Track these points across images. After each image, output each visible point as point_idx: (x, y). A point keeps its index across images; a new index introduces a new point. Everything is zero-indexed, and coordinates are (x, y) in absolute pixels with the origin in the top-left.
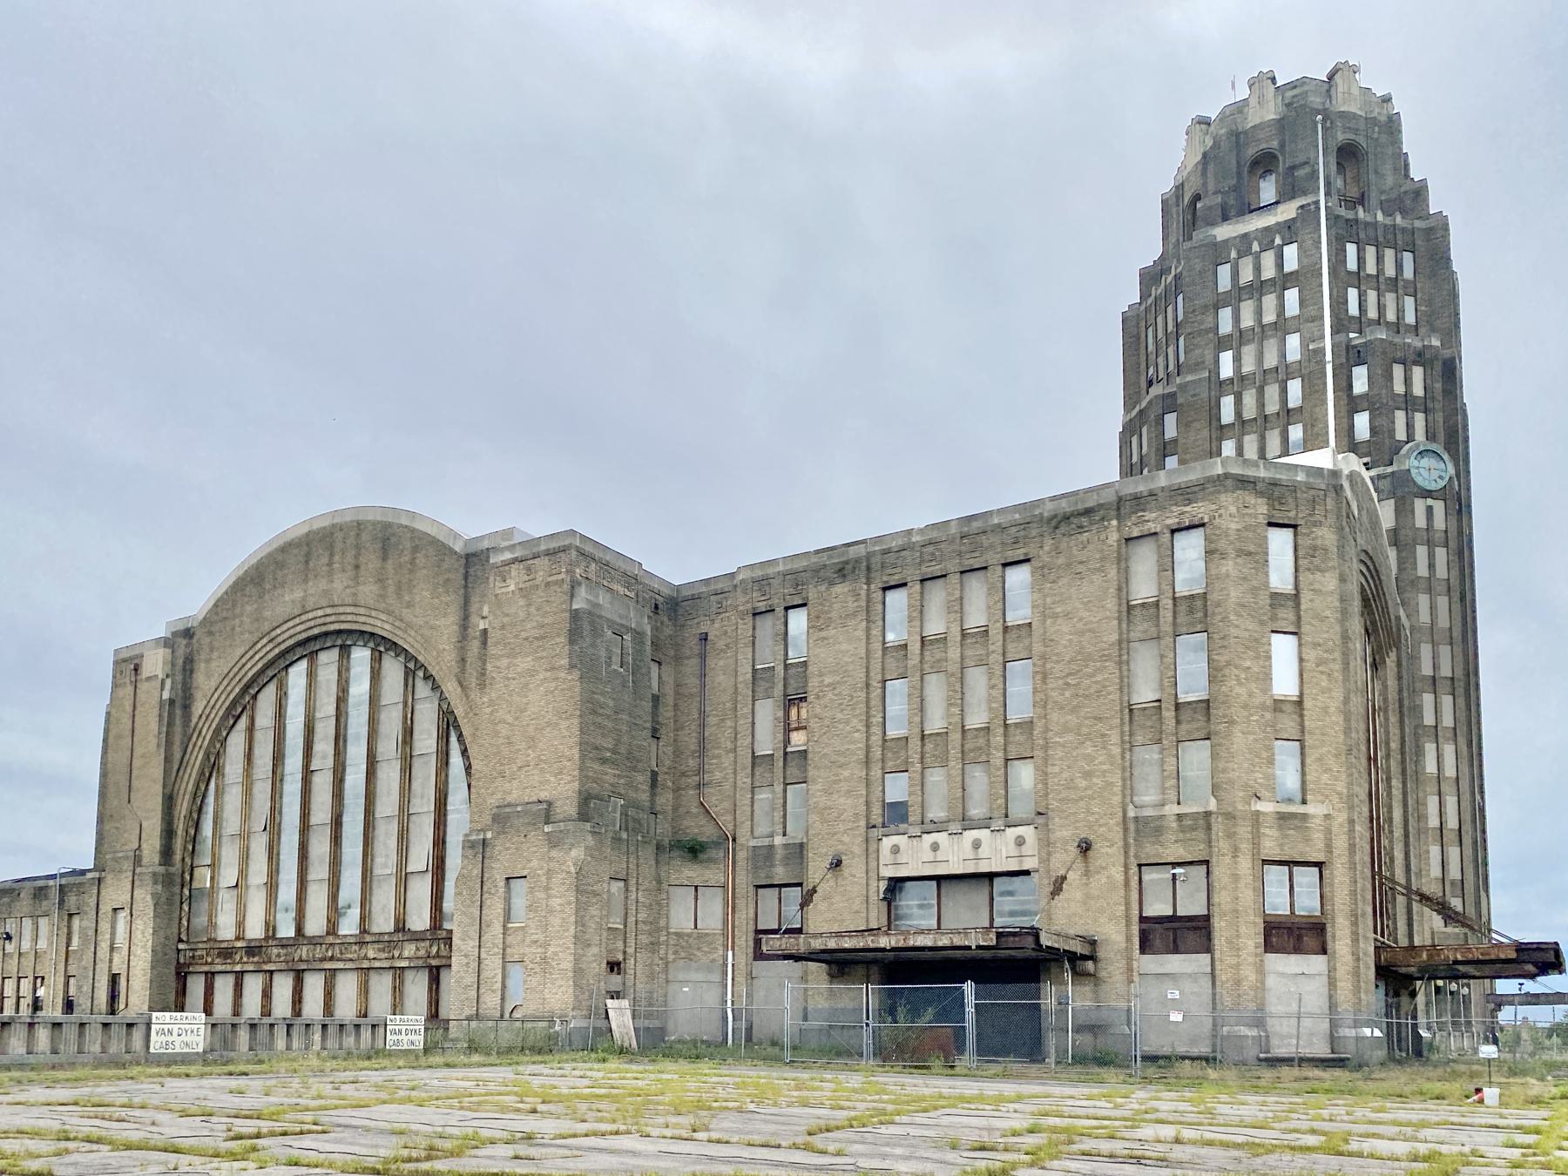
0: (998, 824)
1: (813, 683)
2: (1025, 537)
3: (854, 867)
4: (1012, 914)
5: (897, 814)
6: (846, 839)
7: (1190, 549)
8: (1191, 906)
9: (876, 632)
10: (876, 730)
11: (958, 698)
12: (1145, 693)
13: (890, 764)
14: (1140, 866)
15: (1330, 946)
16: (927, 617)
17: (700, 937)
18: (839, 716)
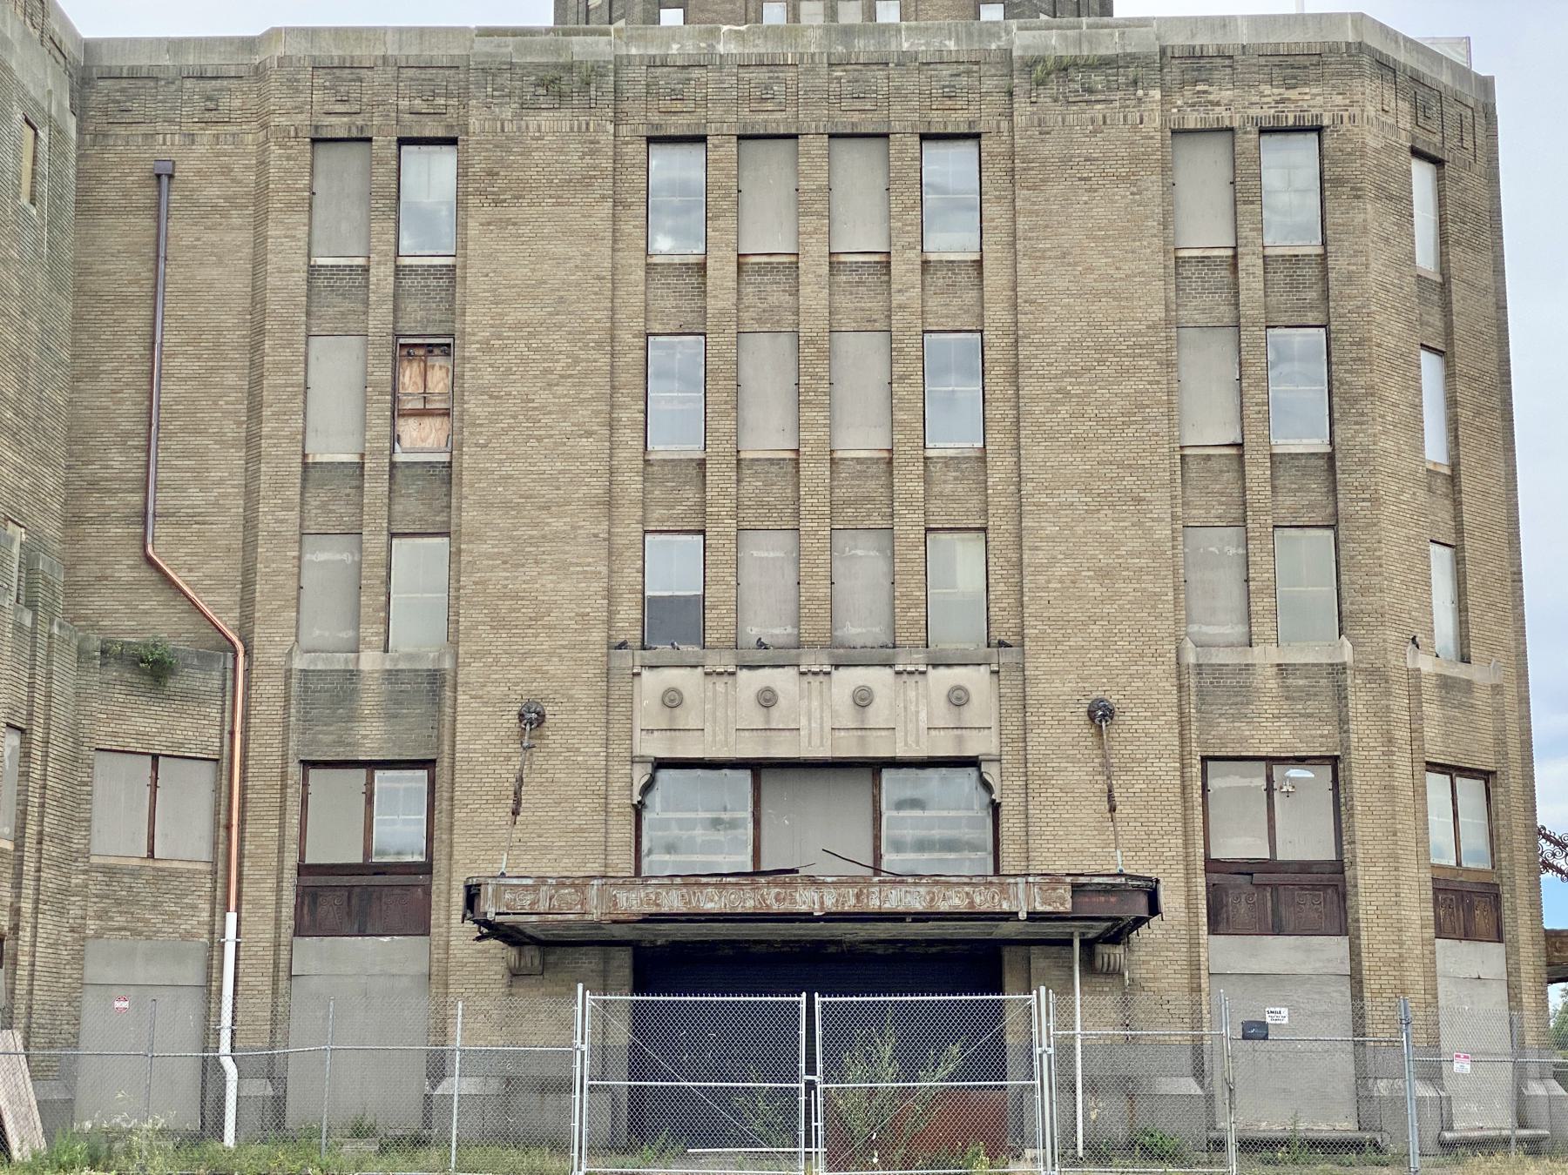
1: (476, 320)
2: (970, 88)
3: (575, 732)
4: (922, 846)
7: (1288, 171)
8: (1304, 839)
9: (631, 227)
10: (629, 437)
12: (1210, 426)
13: (658, 513)
14: (1204, 759)
15: (1507, 928)
17: (162, 876)
18: (542, 397)
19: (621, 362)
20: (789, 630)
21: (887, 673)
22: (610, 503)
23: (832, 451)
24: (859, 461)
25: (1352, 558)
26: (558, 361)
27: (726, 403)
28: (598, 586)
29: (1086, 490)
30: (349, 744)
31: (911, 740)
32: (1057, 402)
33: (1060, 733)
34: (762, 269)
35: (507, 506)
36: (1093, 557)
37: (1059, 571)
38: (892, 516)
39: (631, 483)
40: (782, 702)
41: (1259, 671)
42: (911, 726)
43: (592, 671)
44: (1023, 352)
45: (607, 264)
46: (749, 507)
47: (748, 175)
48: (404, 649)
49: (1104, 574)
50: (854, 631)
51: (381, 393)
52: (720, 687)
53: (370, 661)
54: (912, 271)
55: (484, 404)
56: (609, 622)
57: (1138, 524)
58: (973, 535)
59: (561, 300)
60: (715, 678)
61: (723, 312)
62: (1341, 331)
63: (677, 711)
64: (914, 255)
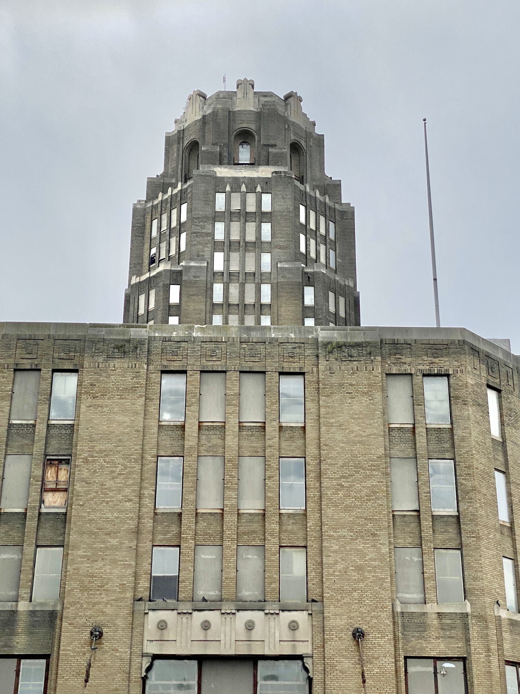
0: (272, 608)
1: (82, 448)
3: (116, 640)
5: (165, 590)
6: (109, 610)
7: (435, 392)
9: (153, 409)
11: (229, 484)
12: (405, 503)
14: (406, 658)
16: (204, 405)
18: (109, 484)
19: (145, 468)
22: (137, 532)
23: (238, 510)
24: (250, 514)
25: (469, 563)
26: (117, 467)
27: (192, 487)
28: (130, 571)
29: (351, 530)
30: (10, 647)
31: (272, 647)
32: (337, 490)
33: (340, 643)
34: (209, 428)
35: (91, 533)
36: (354, 561)
37: (340, 567)
38: (265, 540)
39: (148, 523)
40: (213, 627)
41: (429, 616)
42: (272, 640)
43: (126, 611)
44: (323, 467)
45: (141, 424)
47: (204, 387)
48: (39, 600)
49: (359, 569)
51: (37, 481)
52: (185, 620)
53: (23, 606)
54: (275, 430)
55: (83, 487)
56: (135, 588)
57: (374, 546)
58: (301, 549)
59: (120, 441)
60: (182, 616)
61: (191, 447)
62: (461, 462)
63: (164, 631)
64: (276, 424)
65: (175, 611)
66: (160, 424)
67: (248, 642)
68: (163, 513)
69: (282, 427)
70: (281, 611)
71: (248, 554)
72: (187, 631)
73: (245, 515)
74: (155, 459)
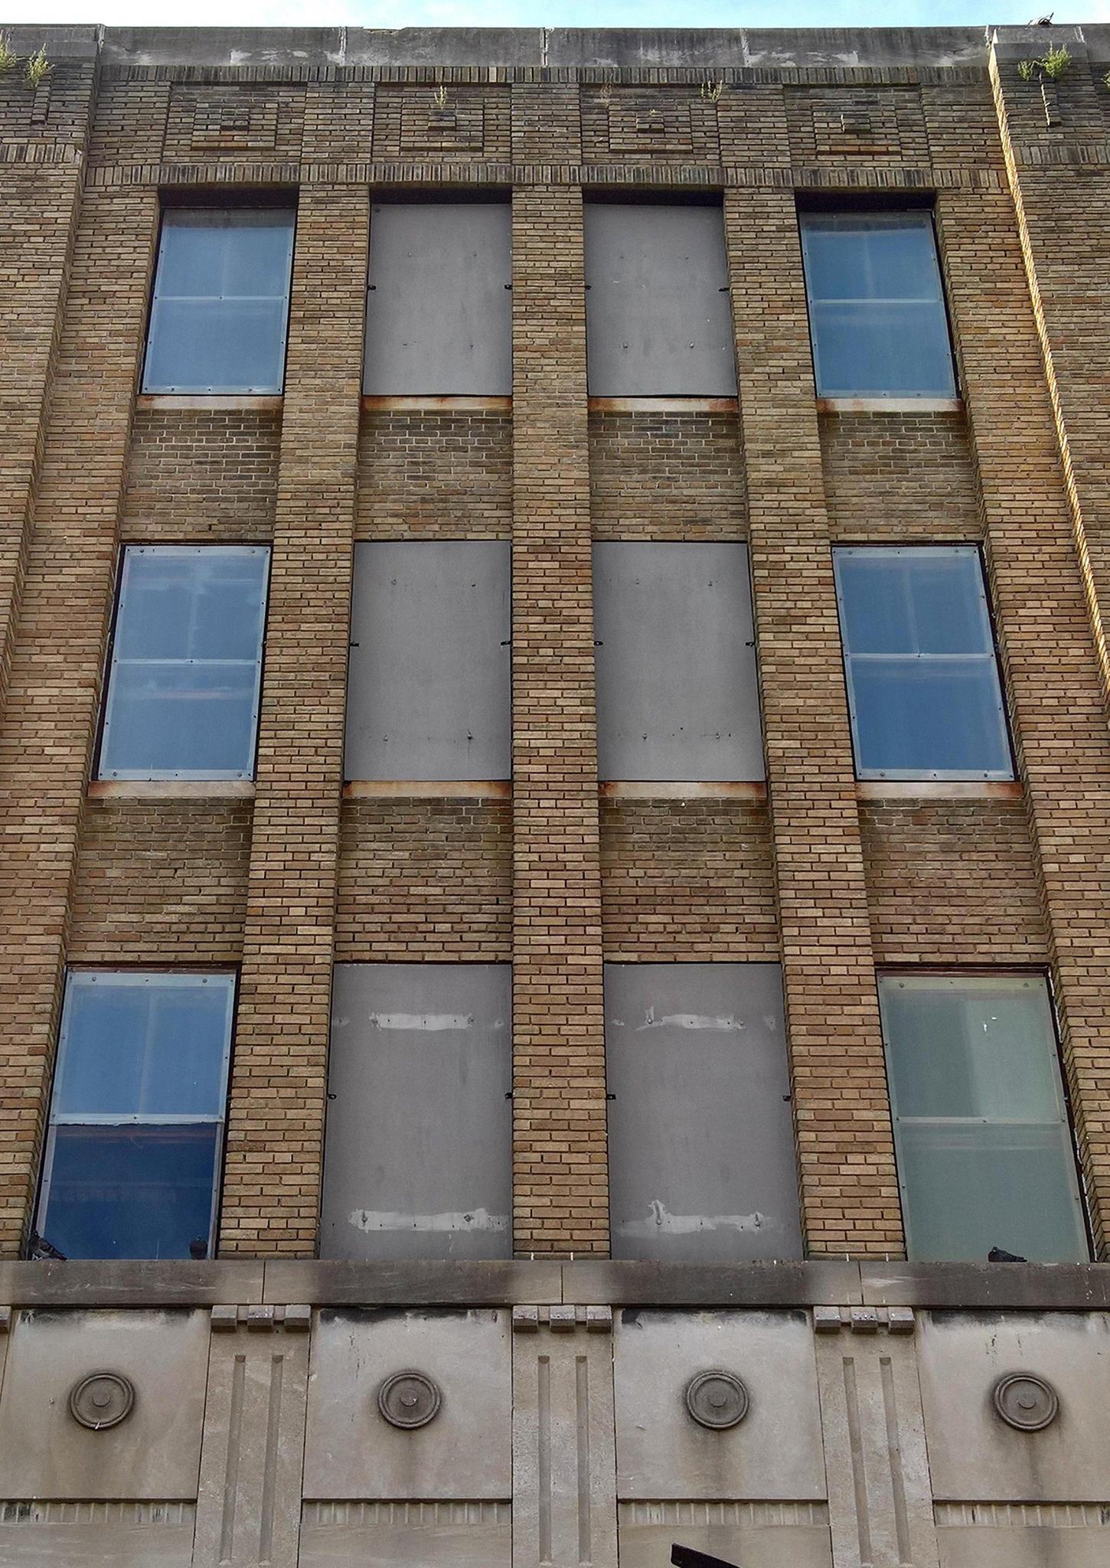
19: (47, 583)
20: (481, 1218)
21: (791, 1337)
23: (603, 784)
27: (317, 667)
34: (414, 423)
38: (776, 932)
40: (459, 1413)
42: (877, 1495)
46: (371, 909)
50: (680, 1224)
52: (258, 1372)
54: (797, 419)
58: (1014, 984)
61: (318, 490)
65: (198, 1318)
66: (143, 404)
67: (707, 1515)
68: (141, 802)
69: (836, 414)
70: (923, 1318)
71: (677, 1010)
72: (271, 1446)
73: (645, 811)
74: (106, 545)
